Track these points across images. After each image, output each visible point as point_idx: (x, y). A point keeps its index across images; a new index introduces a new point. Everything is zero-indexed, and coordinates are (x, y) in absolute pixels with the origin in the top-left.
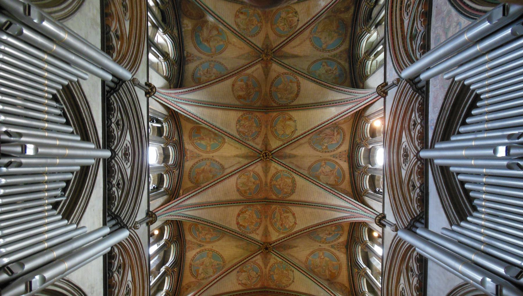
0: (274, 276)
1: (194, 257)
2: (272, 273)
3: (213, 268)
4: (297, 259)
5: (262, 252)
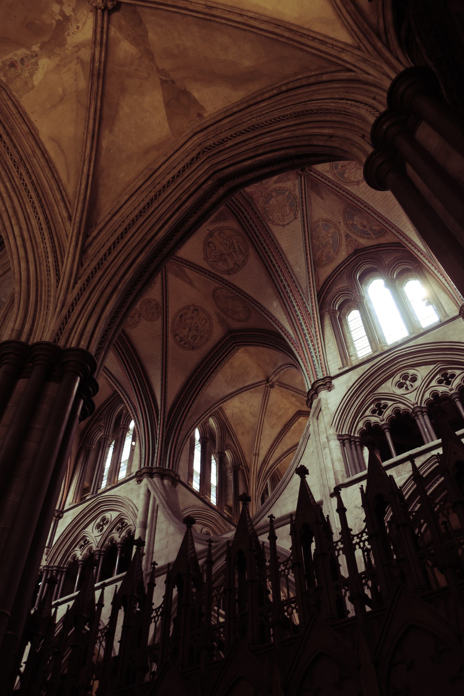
2: (274, 194)
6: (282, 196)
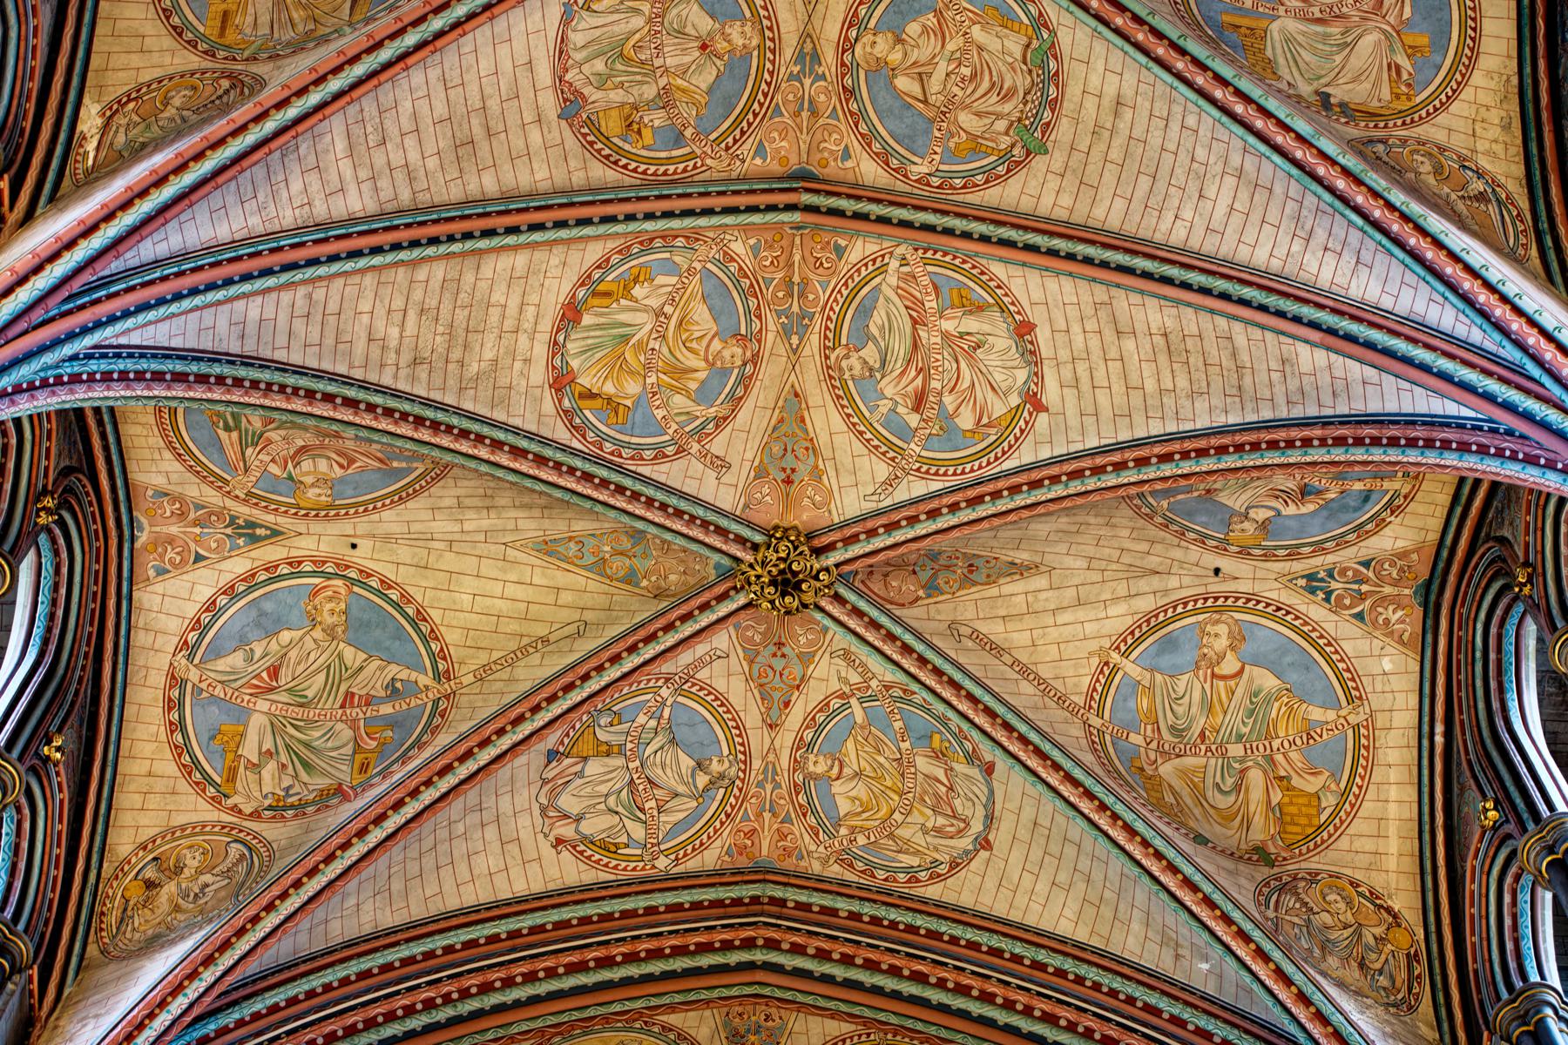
0: (837, 787)
1: (199, 626)
2: (818, 766)
3: (353, 725)
4: (1025, 671)
5: (749, 605)
6: (856, 740)
